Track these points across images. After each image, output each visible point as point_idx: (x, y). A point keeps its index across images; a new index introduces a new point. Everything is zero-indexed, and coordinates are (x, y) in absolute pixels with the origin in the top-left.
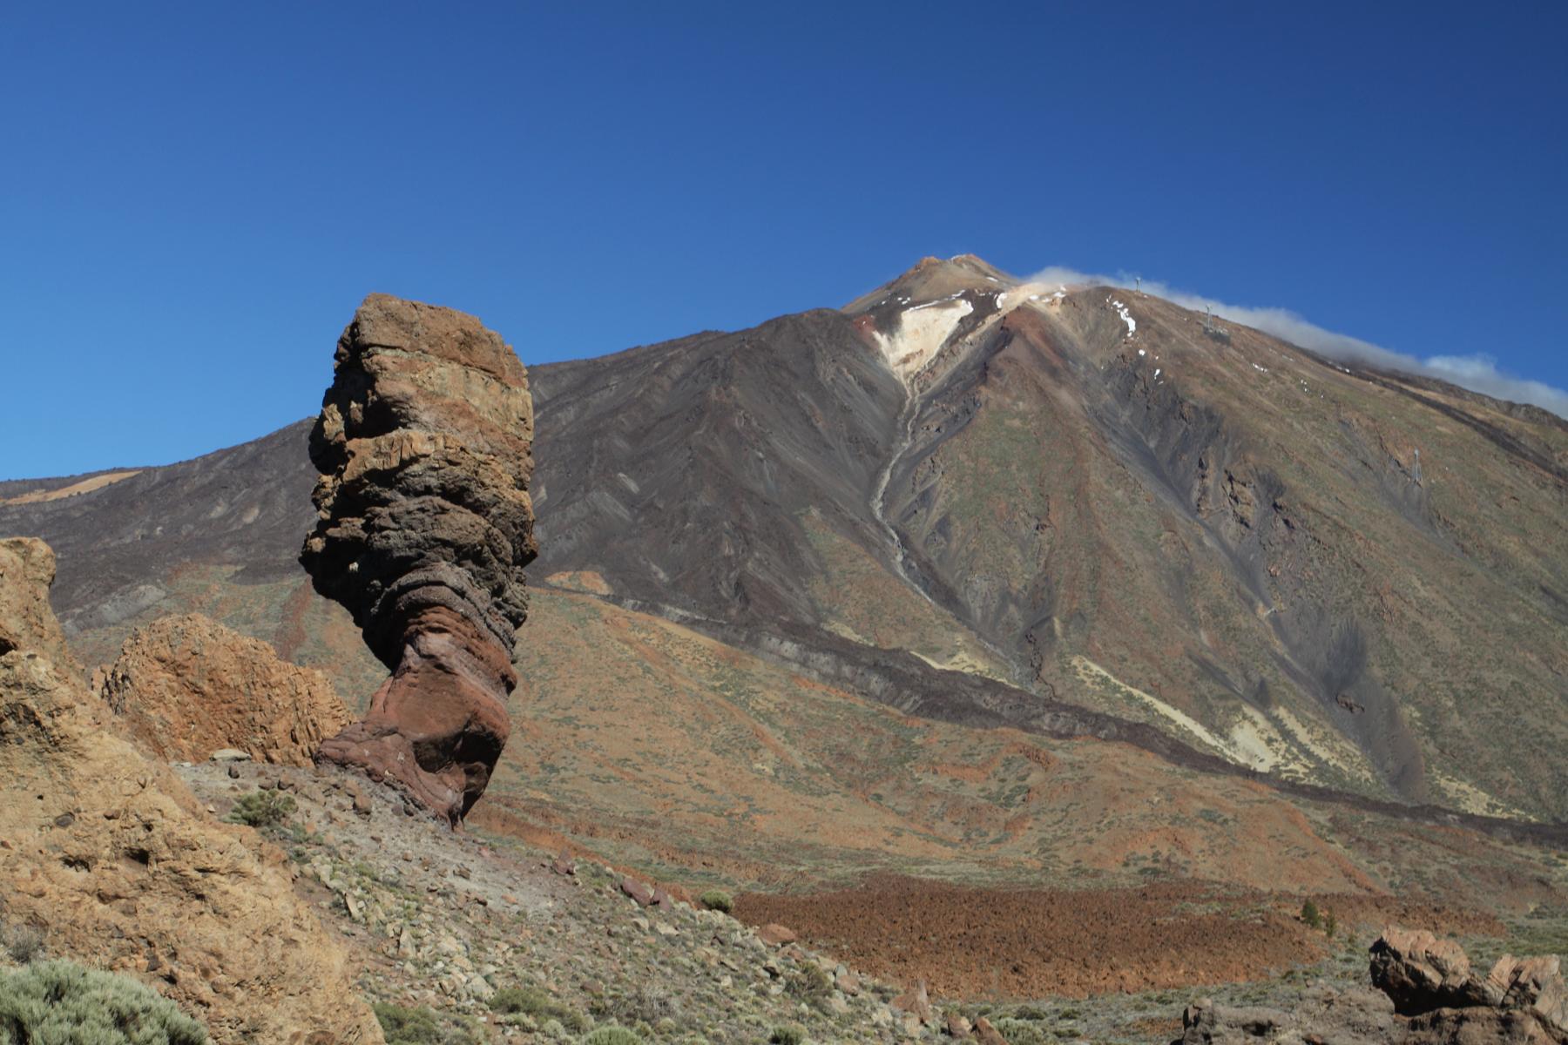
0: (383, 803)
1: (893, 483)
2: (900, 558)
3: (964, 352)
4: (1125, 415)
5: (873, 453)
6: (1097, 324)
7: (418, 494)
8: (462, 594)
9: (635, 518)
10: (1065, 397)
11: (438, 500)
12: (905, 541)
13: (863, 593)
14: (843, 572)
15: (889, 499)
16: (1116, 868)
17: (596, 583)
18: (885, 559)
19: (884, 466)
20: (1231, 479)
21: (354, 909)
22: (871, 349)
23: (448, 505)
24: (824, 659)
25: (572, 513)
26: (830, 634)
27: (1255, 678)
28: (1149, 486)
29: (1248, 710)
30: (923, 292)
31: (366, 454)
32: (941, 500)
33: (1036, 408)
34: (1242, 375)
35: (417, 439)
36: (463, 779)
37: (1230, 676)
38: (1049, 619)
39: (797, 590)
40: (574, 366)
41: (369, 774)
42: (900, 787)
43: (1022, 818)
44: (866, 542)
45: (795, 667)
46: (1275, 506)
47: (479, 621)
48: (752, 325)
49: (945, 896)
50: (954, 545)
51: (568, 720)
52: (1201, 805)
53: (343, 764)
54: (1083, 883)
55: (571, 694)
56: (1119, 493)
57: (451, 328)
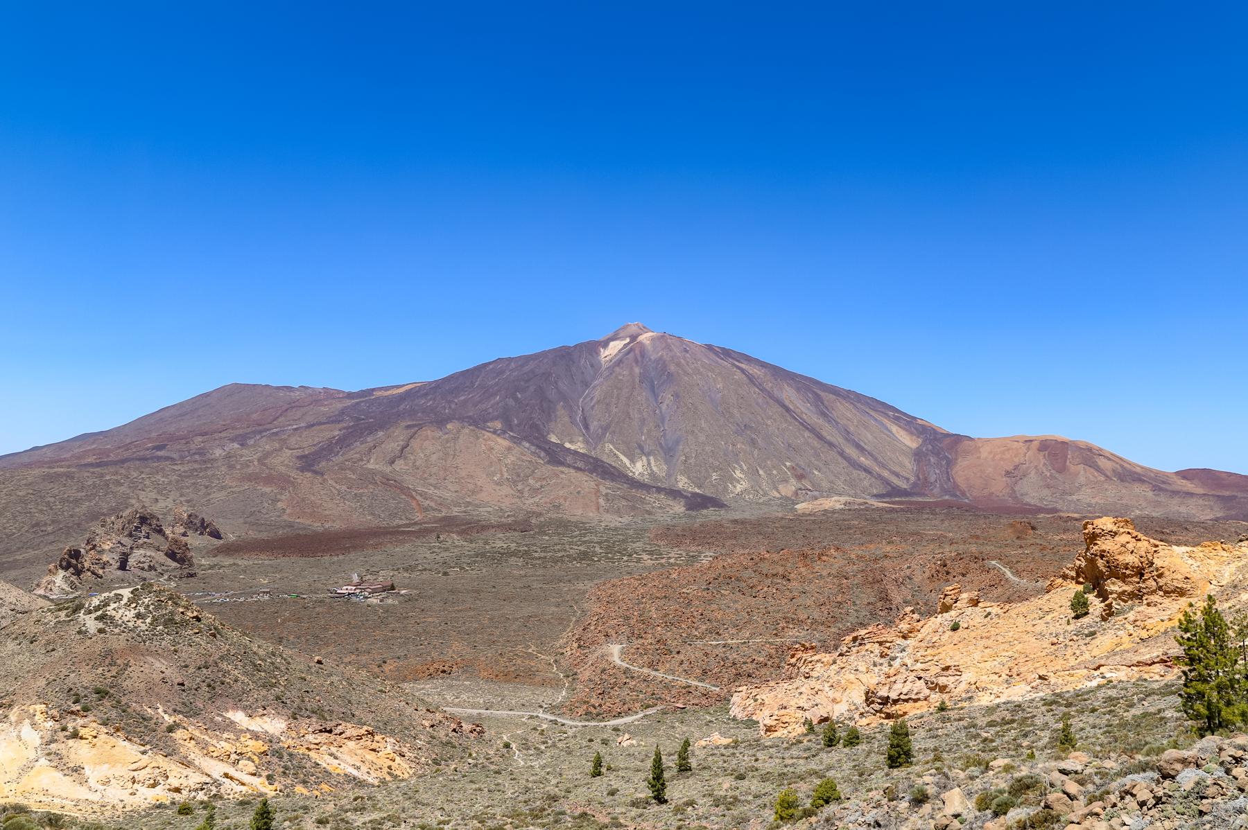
5: (586, 384)
22: (598, 354)
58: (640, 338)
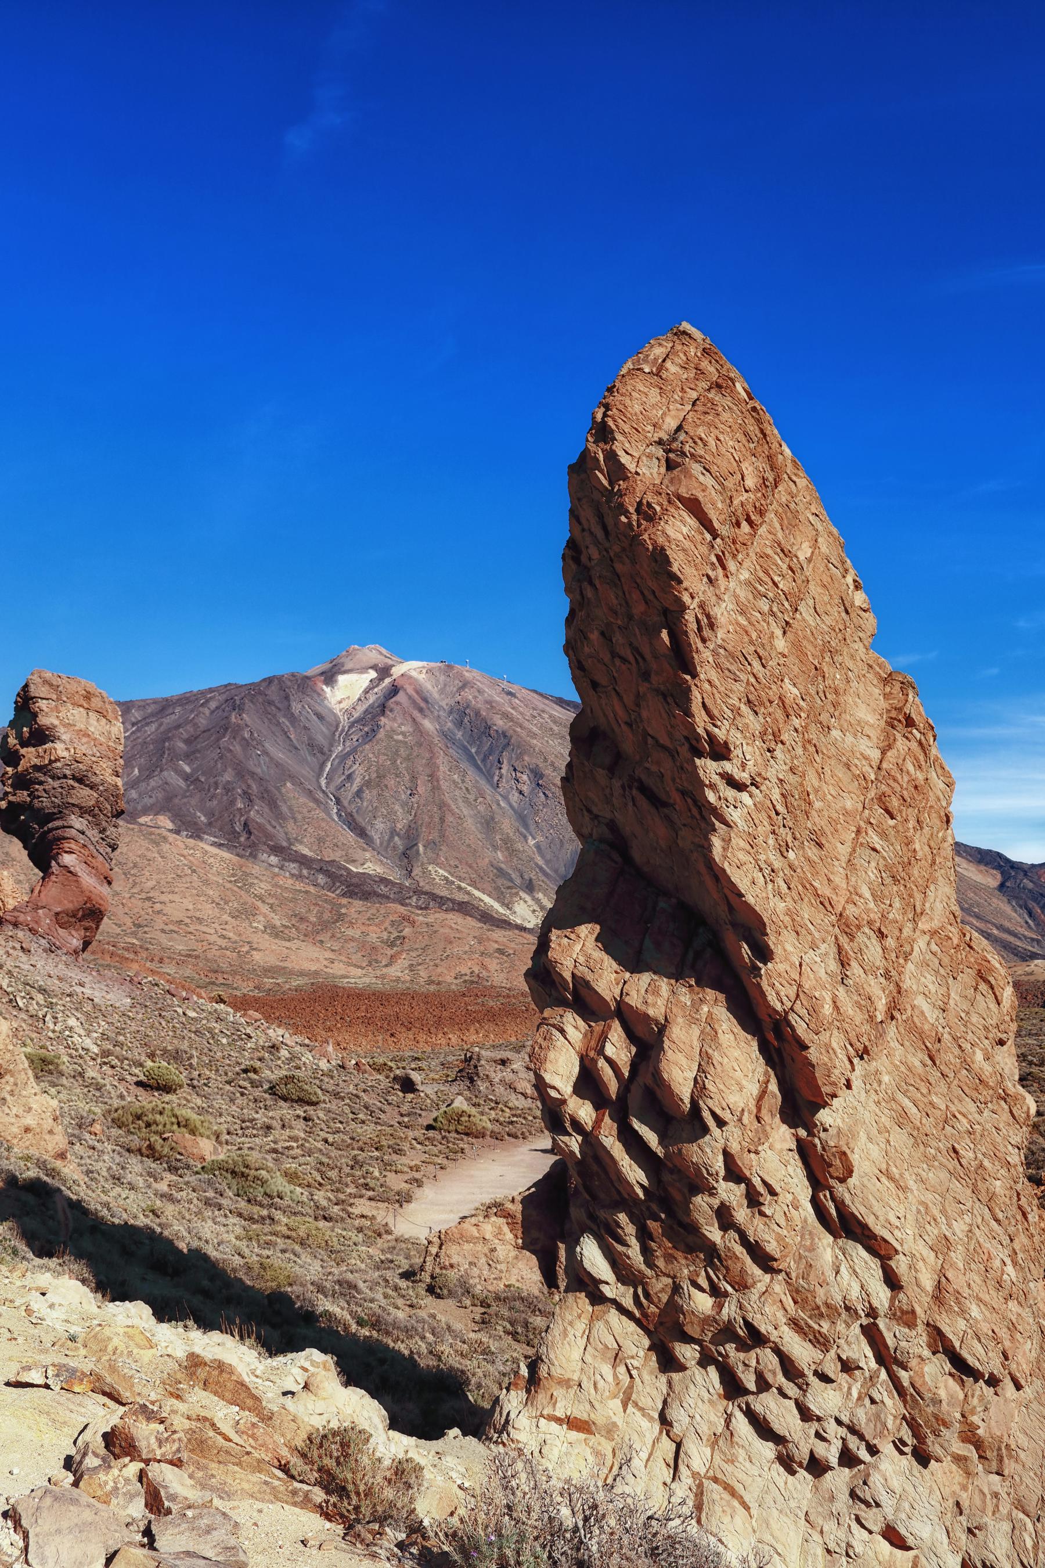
0: (37, 946)
1: (333, 770)
2: (335, 810)
3: (372, 699)
4: (459, 735)
5: (321, 752)
6: (445, 685)
7: (59, 778)
8: (83, 833)
9: (189, 786)
10: (428, 724)
11: (71, 782)
12: (338, 801)
13: (314, 828)
14: (304, 818)
15: (330, 779)
16: (449, 979)
17: (165, 822)
18: (327, 811)
19: (328, 759)
20: (515, 770)
21: (21, 1004)
22: (320, 694)
23: (76, 785)
24: (292, 865)
25: (153, 783)
26: (296, 851)
27: (526, 877)
28: (472, 774)
29: (521, 894)
30: (349, 666)
31: (30, 756)
32: (358, 780)
33: (411, 730)
34: (521, 714)
35: (60, 749)
36: (82, 932)
37: (513, 876)
38: (416, 844)
39: (278, 827)
40: (155, 702)
41: (30, 930)
42: (333, 936)
43: (400, 953)
44: (317, 801)
45: (277, 870)
46: (538, 784)
47: (92, 847)
48: (257, 680)
49: (357, 995)
50: (365, 804)
51: (149, 899)
52: (496, 946)
53: (16, 925)
54: (432, 988)
55: (150, 884)
56: (456, 776)
57: (79, 689)
58: (397, 671)
